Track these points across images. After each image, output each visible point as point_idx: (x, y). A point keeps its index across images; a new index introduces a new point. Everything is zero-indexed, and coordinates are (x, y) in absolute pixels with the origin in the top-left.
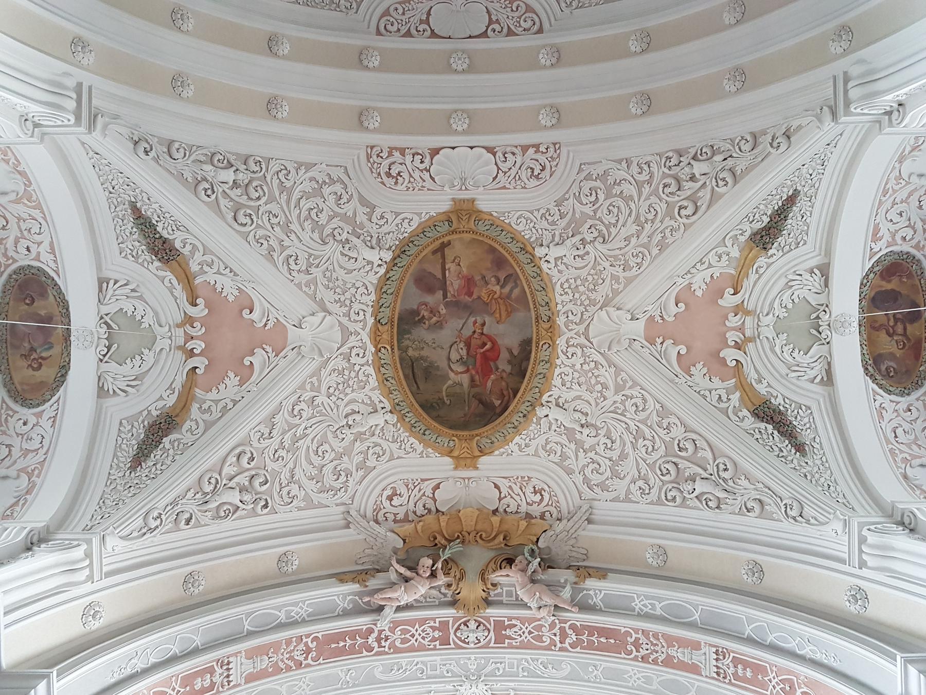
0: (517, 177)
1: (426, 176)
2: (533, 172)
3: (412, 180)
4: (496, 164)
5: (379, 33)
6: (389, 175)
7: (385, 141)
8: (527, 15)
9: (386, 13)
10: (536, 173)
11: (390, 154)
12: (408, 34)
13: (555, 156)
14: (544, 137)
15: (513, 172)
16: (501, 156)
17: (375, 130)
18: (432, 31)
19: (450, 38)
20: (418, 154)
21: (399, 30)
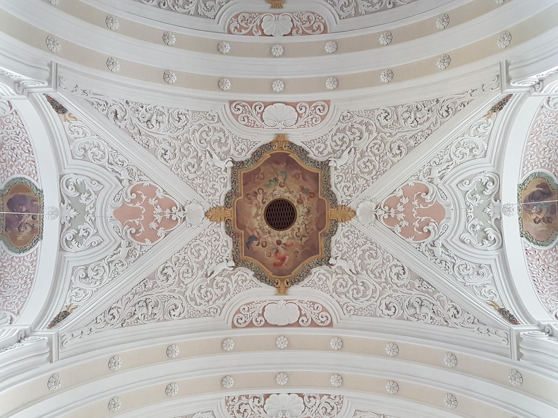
0: (317, 412)
1: (261, 410)
2: (326, 409)
3: (253, 413)
4: (304, 403)
5: (234, 327)
6: (239, 412)
7: (236, 394)
8: (323, 313)
9: (238, 312)
10: (328, 411)
11: (240, 398)
12: (251, 325)
13: (340, 402)
14: (333, 393)
15: (314, 409)
16: (307, 398)
17: (232, 389)
18: (266, 321)
19: (276, 326)
20: (257, 398)
21: (245, 321)
